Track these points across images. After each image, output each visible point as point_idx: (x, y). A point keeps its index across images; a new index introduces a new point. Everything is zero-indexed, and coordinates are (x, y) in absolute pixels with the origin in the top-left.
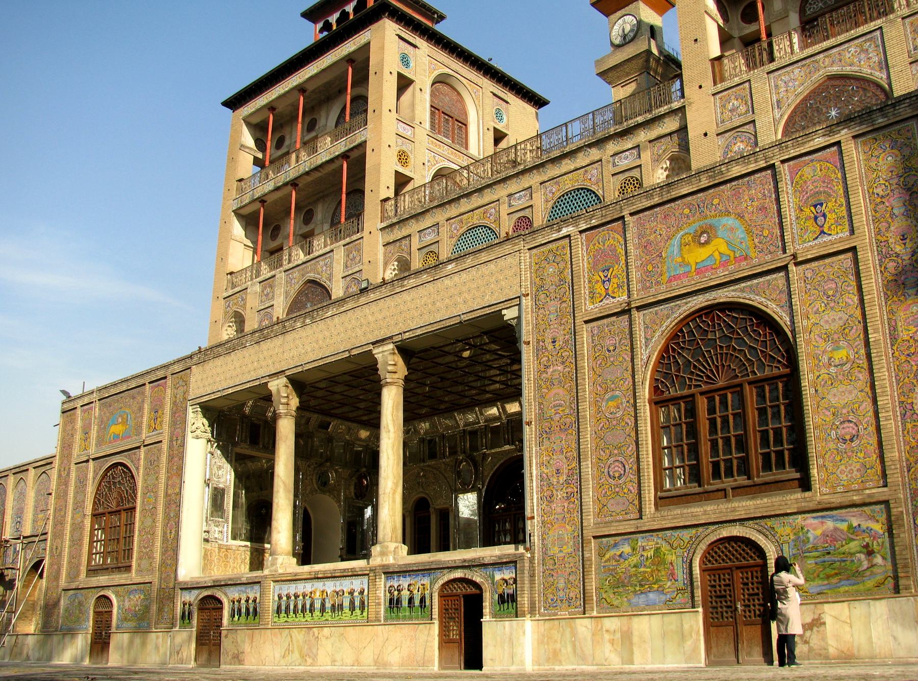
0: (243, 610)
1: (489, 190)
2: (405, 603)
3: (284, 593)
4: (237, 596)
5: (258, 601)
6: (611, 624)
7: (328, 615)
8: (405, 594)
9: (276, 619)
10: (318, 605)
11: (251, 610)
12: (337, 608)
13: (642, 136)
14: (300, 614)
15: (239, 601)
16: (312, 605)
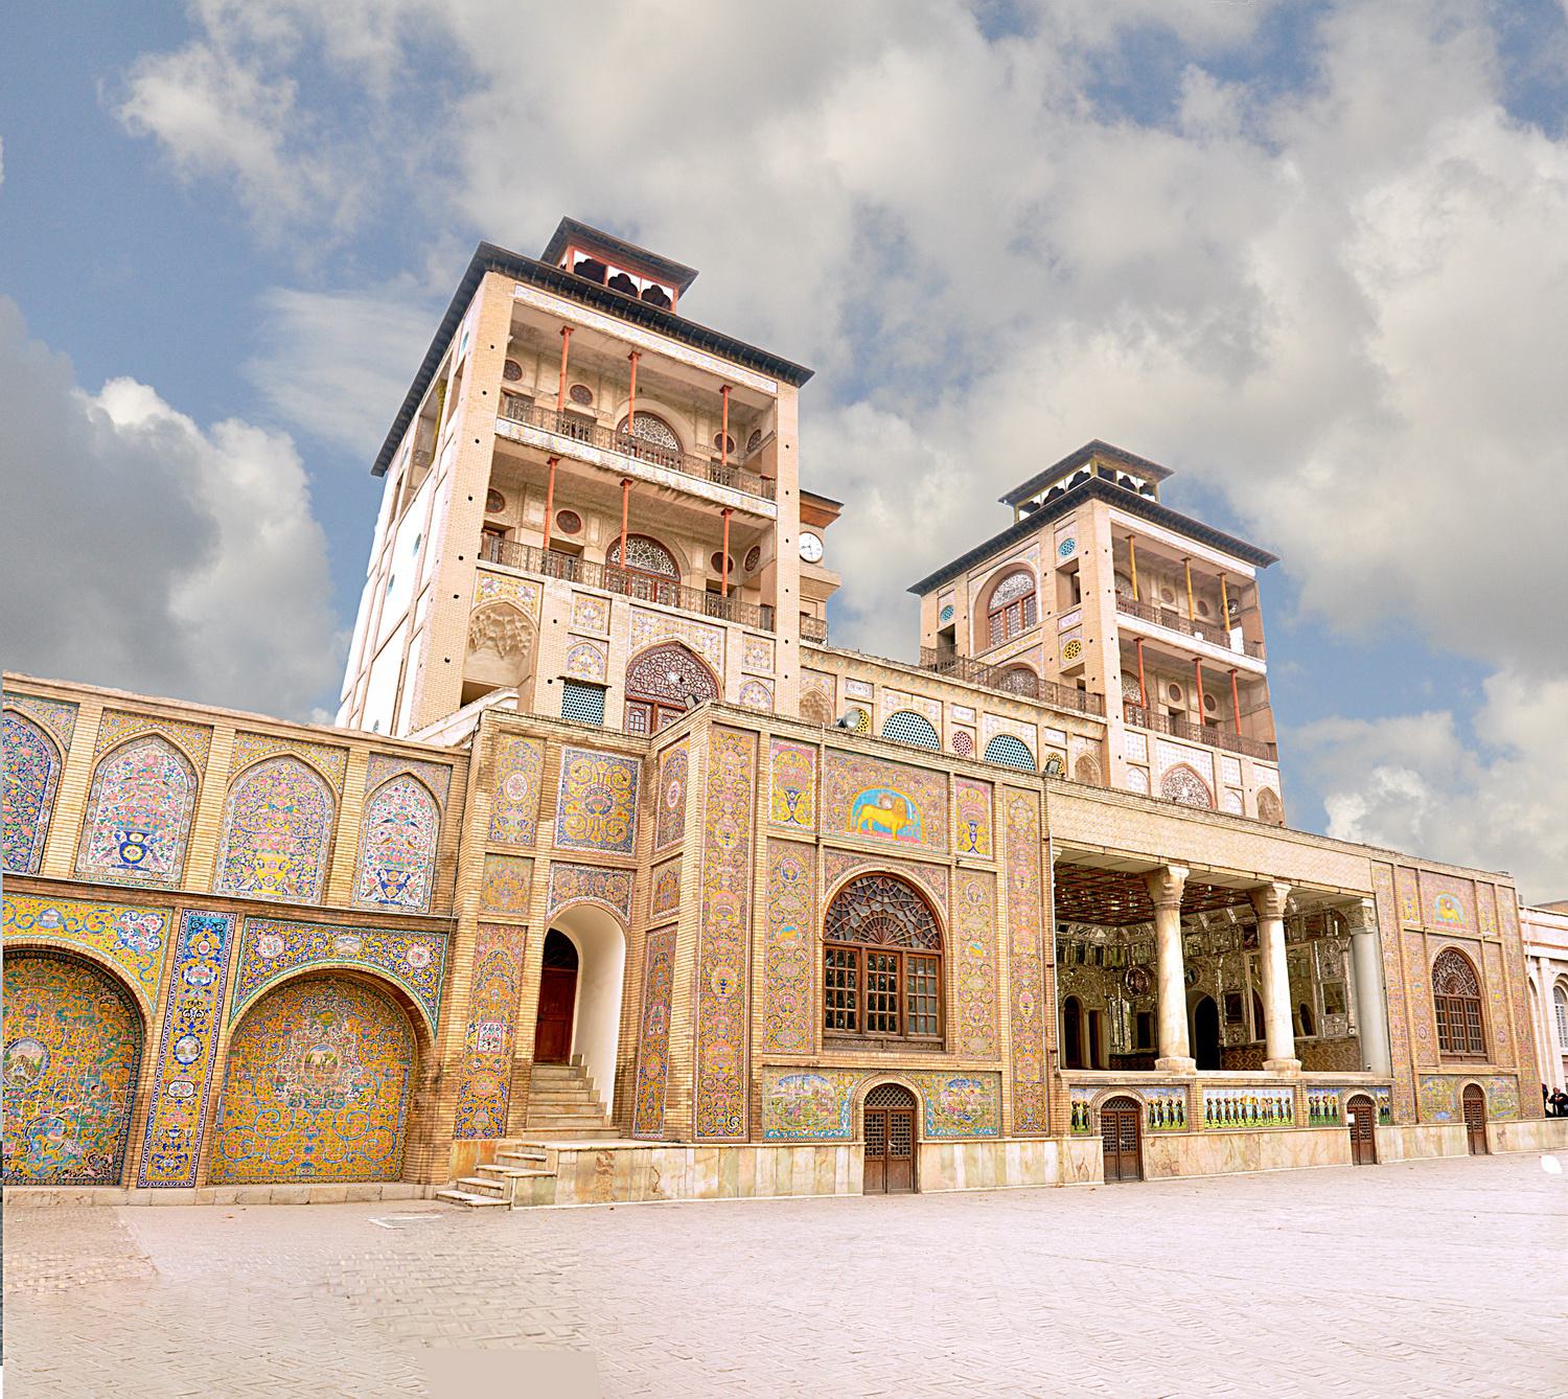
0: (1166, 1115)
1: (936, 686)
2: (1322, 1112)
3: (1213, 1099)
4: (1155, 1099)
5: (1184, 1104)
6: (1432, 1131)
7: (1259, 1122)
8: (1321, 1104)
9: (1208, 1125)
10: (1249, 1111)
11: (1176, 1115)
12: (1268, 1115)
13: (1071, 727)
14: (1241, 1121)
15: (1160, 1105)
16: (1244, 1111)
